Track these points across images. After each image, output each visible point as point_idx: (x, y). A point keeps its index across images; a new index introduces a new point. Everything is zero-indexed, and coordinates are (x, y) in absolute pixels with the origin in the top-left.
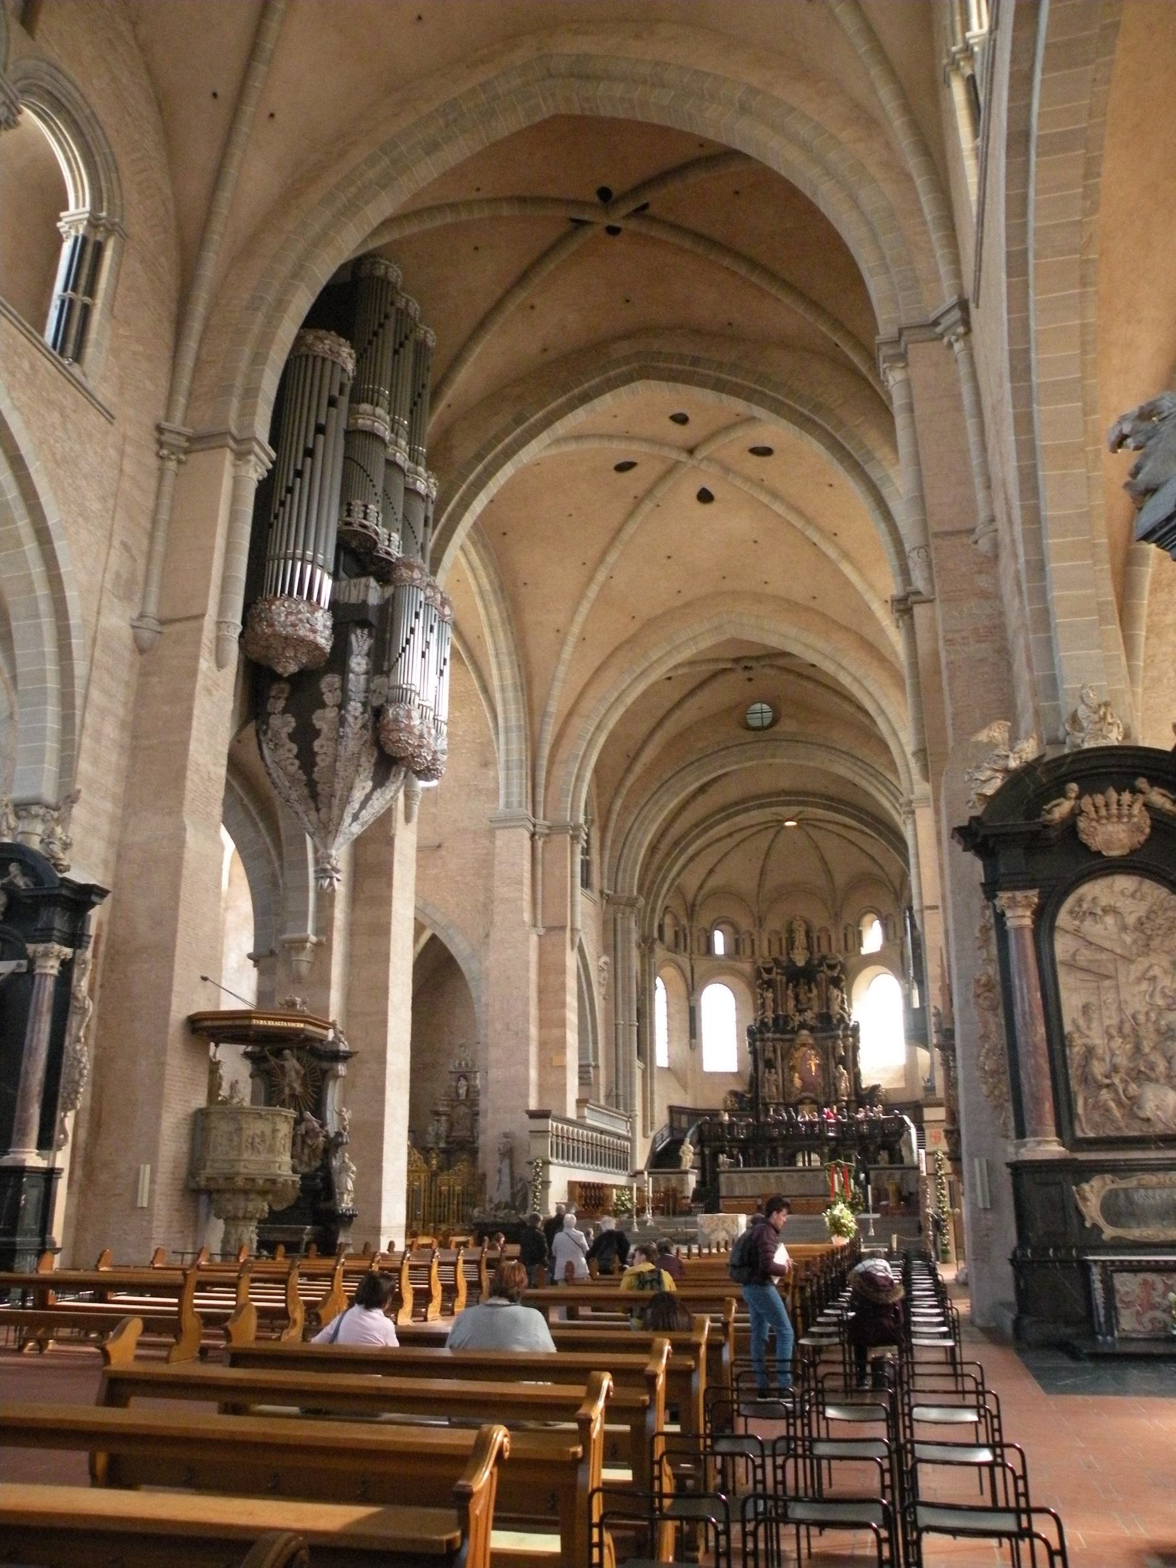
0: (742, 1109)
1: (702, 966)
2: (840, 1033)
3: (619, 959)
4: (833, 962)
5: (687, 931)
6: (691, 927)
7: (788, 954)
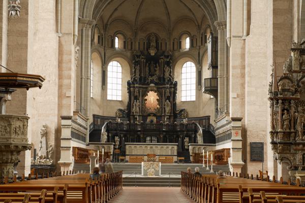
0: (123, 117)
1: (109, 52)
2: (169, 86)
3: (84, 48)
4: (166, 54)
5: (103, 36)
6: (105, 34)
7: (147, 50)
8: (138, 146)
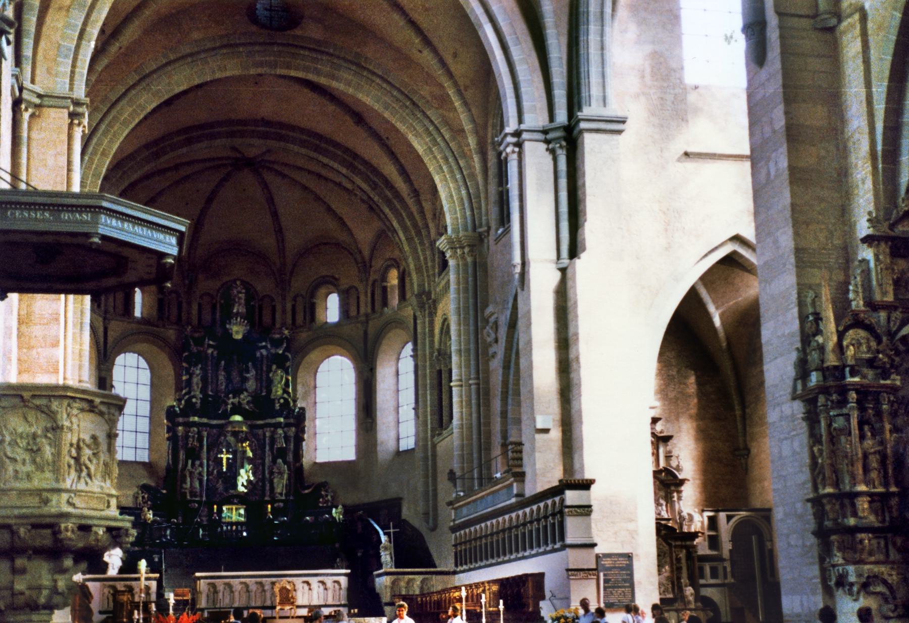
1: (117, 328)
8: (235, 582)
